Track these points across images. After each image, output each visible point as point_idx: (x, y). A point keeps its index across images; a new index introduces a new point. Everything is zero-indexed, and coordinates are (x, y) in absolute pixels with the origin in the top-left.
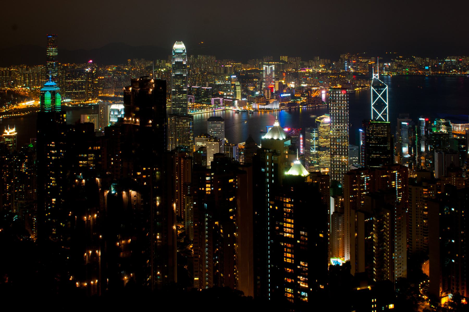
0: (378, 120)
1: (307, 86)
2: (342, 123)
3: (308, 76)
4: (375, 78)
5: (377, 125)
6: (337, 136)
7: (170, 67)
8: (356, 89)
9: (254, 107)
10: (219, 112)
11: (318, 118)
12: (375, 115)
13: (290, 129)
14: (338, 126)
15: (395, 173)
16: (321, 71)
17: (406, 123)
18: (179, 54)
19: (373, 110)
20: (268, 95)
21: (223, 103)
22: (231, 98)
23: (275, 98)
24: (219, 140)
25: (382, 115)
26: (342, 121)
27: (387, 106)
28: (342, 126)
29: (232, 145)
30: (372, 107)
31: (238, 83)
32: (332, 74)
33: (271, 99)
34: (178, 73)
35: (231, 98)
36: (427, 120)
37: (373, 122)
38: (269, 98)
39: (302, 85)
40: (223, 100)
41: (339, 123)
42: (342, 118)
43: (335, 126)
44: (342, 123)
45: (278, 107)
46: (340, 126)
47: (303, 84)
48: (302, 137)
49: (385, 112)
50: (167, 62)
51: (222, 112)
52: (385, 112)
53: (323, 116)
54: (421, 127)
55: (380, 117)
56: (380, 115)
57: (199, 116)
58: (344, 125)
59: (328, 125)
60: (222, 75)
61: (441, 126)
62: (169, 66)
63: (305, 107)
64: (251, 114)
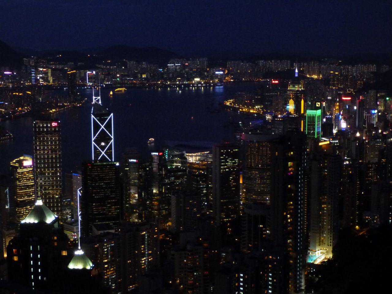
0: (100, 161)
2: (52, 167)
5: (102, 167)
6: (46, 186)
8: (51, 111)
11: (14, 161)
12: (97, 154)
15: (145, 234)
17: (135, 161)
19: (94, 146)
25: (105, 153)
26: (52, 165)
28: (53, 171)
30: (93, 143)
32: (14, 90)
36: (161, 154)
37: (97, 164)
41: (48, 168)
42: (52, 161)
44: (52, 167)
46: (50, 172)
49: (110, 148)
52: (110, 148)
53: (22, 158)
54: (153, 163)
55: (103, 156)
59: (29, 171)
61: (174, 159)
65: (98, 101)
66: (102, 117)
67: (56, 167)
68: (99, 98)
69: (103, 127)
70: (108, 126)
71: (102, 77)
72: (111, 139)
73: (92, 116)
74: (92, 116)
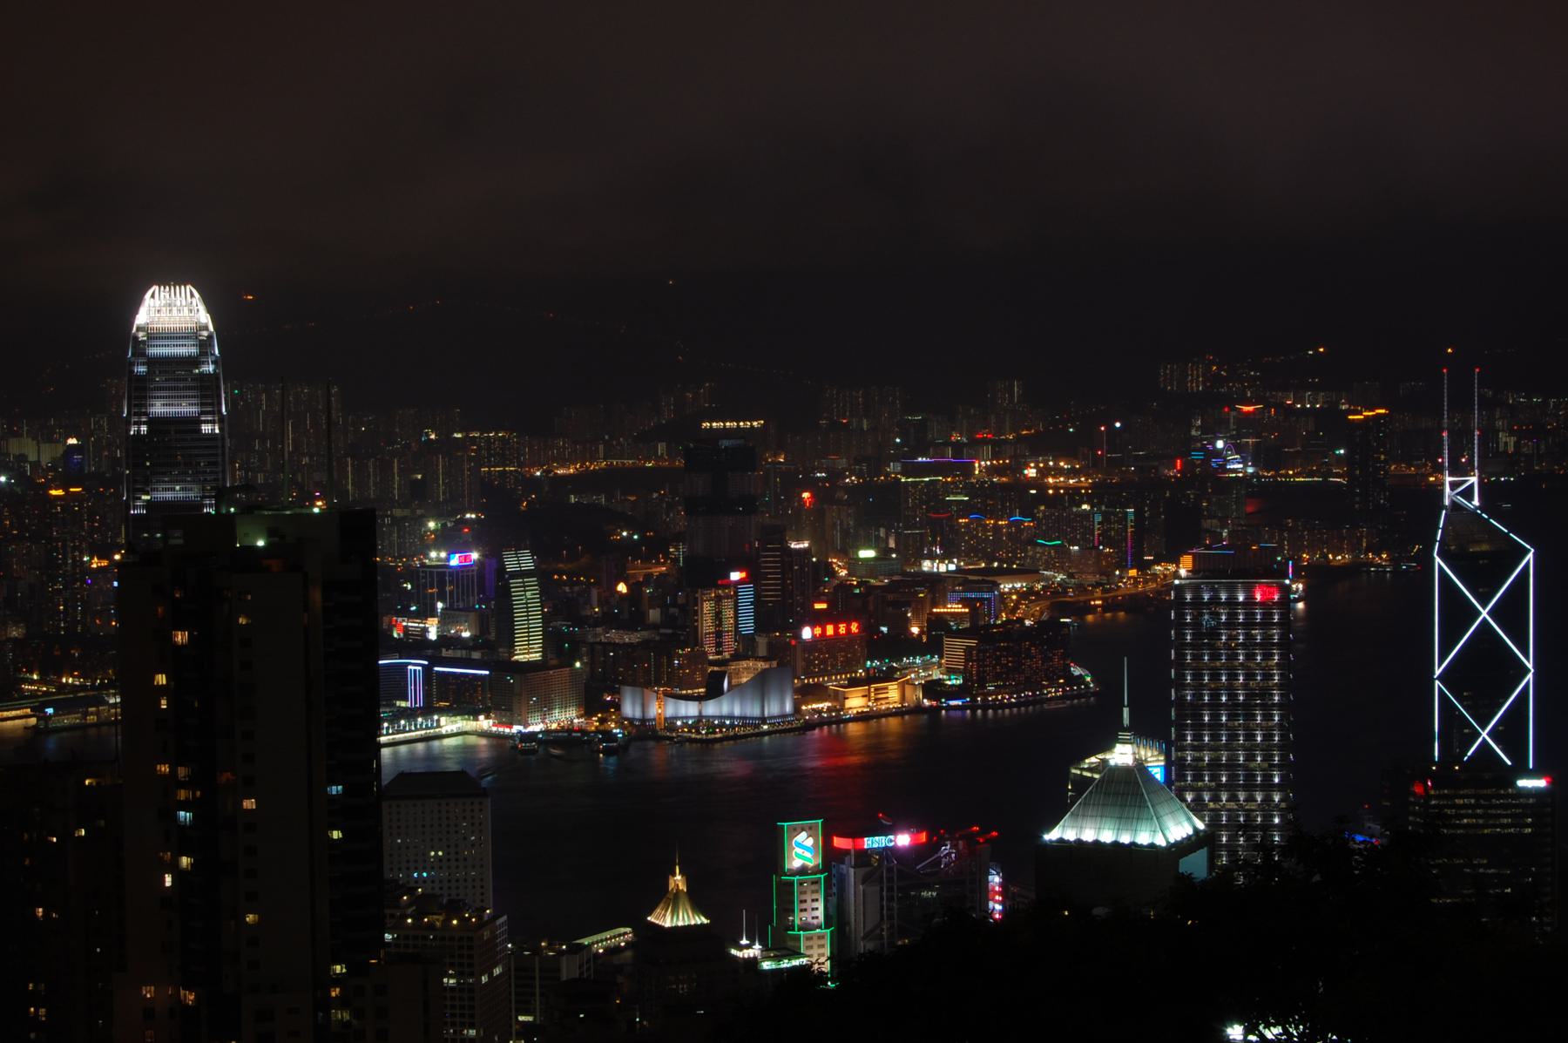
1: (959, 570)
2: (1250, 787)
3: (964, 509)
4: (1454, 504)
7: (36, 465)
9: (630, 709)
10: (403, 749)
12: (1458, 734)
13: (923, 837)
14: (1232, 805)
16: (1039, 471)
18: (175, 372)
20: (719, 634)
21: (427, 695)
22: (476, 655)
23: (762, 651)
24: (480, 918)
27: (1530, 676)
28: (1252, 806)
29: (549, 948)
31: (527, 561)
33: (736, 657)
34: (169, 495)
35: (476, 655)
38: (727, 655)
39: (926, 565)
40: (427, 670)
41: (1231, 787)
43: (1212, 805)
44: (1250, 787)
45: (788, 708)
47: (932, 557)
48: (1001, 885)
50: (17, 435)
51: (420, 746)
56: (1484, 734)
57: (412, 753)
58: (1268, 799)
60: (398, 513)
62: (32, 458)
63: (959, 703)
64: (612, 760)
65: (1468, 494)
66: (1484, 575)
67: (1268, 786)
68: (1474, 480)
69: (1484, 613)
70: (1510, 613)
71: (1506, 443)
72: (1526, 671)
73: (1438, 560)
74: (1438, 560)
